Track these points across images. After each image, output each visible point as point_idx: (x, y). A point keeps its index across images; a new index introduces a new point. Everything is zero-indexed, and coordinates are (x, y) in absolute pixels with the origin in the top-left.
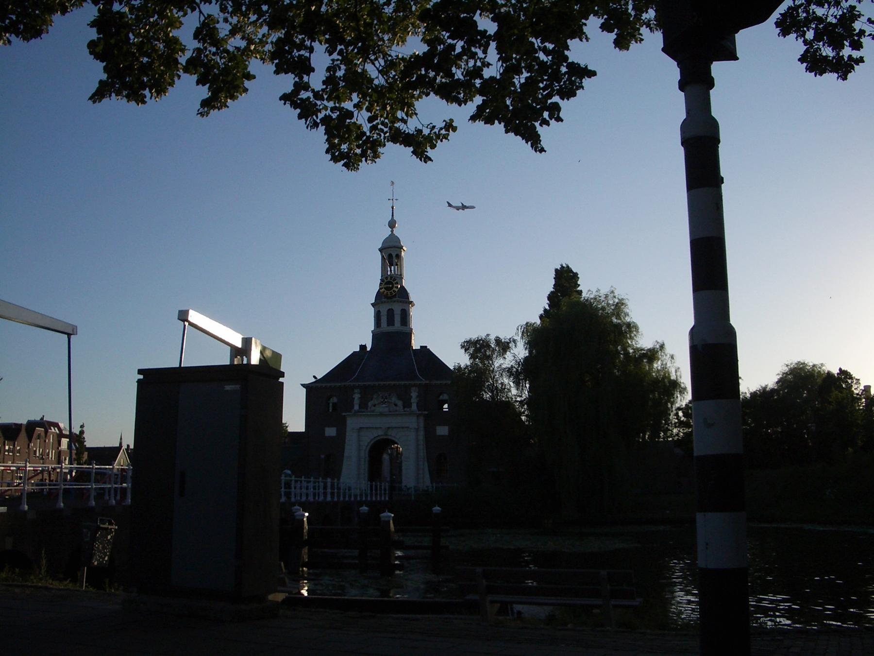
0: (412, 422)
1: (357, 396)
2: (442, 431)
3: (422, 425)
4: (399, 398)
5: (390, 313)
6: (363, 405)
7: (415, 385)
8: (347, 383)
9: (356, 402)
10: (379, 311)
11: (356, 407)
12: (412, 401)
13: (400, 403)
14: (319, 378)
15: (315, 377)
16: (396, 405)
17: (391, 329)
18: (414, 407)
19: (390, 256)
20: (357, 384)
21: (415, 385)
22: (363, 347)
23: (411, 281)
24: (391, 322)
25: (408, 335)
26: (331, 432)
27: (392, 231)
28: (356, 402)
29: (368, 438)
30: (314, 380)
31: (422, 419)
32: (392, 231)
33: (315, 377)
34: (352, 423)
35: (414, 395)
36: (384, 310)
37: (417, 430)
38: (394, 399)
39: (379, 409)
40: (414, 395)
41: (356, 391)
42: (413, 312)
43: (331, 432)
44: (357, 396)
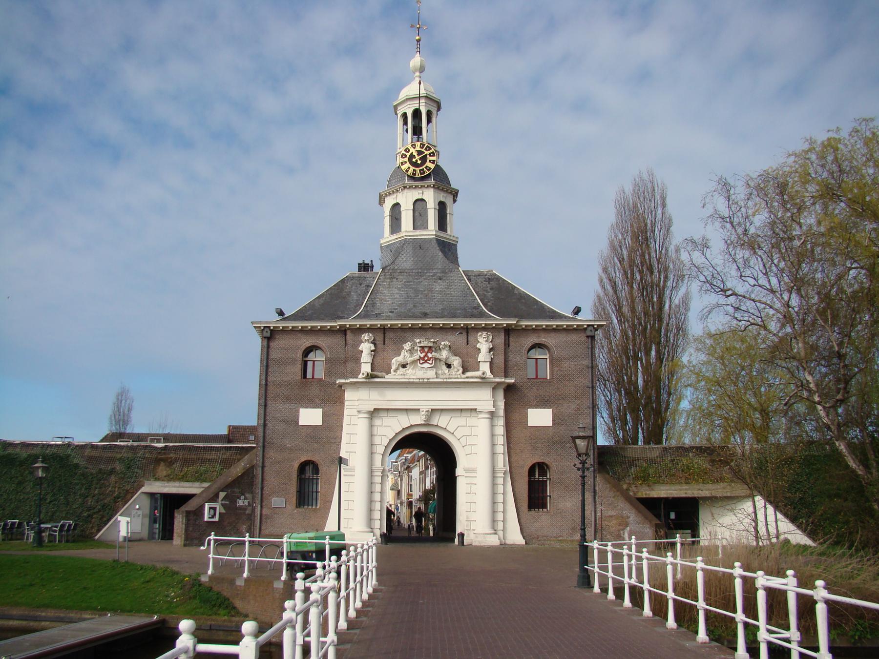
0: (485, 400)
1: (366, 348)
2: (540, 417)
3: (501, 404)
4: (454, 351)
6: (379, 365)
7: (486, 328)
8: (347, 323)
9: (366, 358)
12: (481, 357)
13: (456, 362)
15: (281, 313)
16: (449, 366)
17: (420, 234)
18: (485, 368)
20: (368, 323)
21: (486, 328)
24: (419, 220)
26: (310, 417)
28: (366, 358)
29: (392, 428)
31: (501, 394)
33: (281, 313)
34: (356, 401)
35: (483, 344)
37: (492, 415)
39: (414, 373)
40: (483, 344)
41: (366, 336)
43: (310, 417)
44: (366, 348)
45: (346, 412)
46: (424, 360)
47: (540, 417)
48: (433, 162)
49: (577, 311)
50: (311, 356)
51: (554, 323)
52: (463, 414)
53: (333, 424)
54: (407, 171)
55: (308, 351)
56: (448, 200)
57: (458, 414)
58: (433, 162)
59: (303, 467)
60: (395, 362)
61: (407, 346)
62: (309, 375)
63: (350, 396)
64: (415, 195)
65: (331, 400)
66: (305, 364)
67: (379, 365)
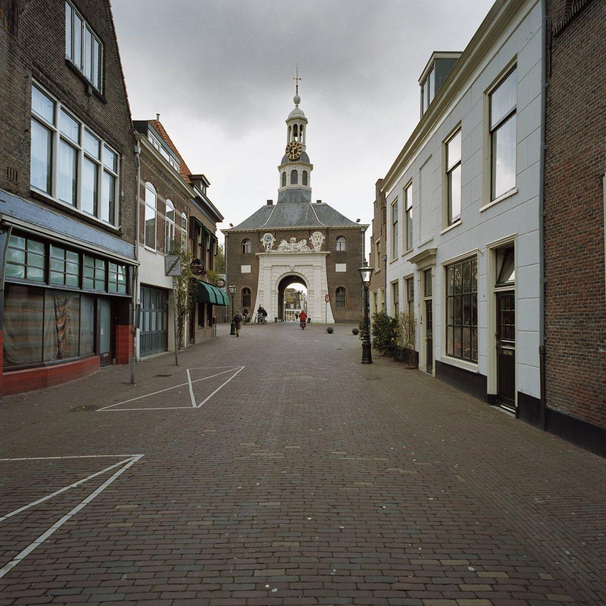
2: (341, 268)
5: (294, 172)
10: (284, 173)
14: (235, 225)
15: (231, 225)
17: (294, 186)
19: (295, 126)
22: (270, 202)
23: (312, 149)
24: (294, 180)
25: (309, 192)
27: (297, 106)
30: (230, 227)
32: (297, 106)
33: (231, 225)
34: (264, 263)
36: (288, 170)
42: (313, 175)
43: (246, 269)
45: (260, 267)
48: (300, 152)
49: (358, 221)
50: (246, 244)
52: (309, 267)
54: (289, 156)
55: (245, 241)
56: (307, 169)
57: (306, 267)
58: (300, 152)
59: (245, 290)
62: (246, 252)
63: (261, 260)
64: (292, 168)
65: (254, 261)
66: (244, 246)
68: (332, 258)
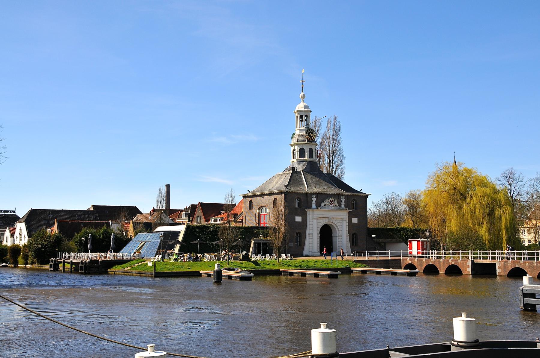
1: (314, 200)
2: (355, 220)
6: (318, 205)
11: (314, 206)
17: (311, 160)
24: (311, 156)
26: (298, 219)
35: (343, 200)
38: (336, 203)
43: (298, 219)
44: (314, 200)
46: (331, 204)
47: (355, 220)
51: (357, 194)
53: (305, 221)
60: (323, 204)
61: (327, 200)
65: (304, 215)
67: (318, 205)
68: (351, 215)
